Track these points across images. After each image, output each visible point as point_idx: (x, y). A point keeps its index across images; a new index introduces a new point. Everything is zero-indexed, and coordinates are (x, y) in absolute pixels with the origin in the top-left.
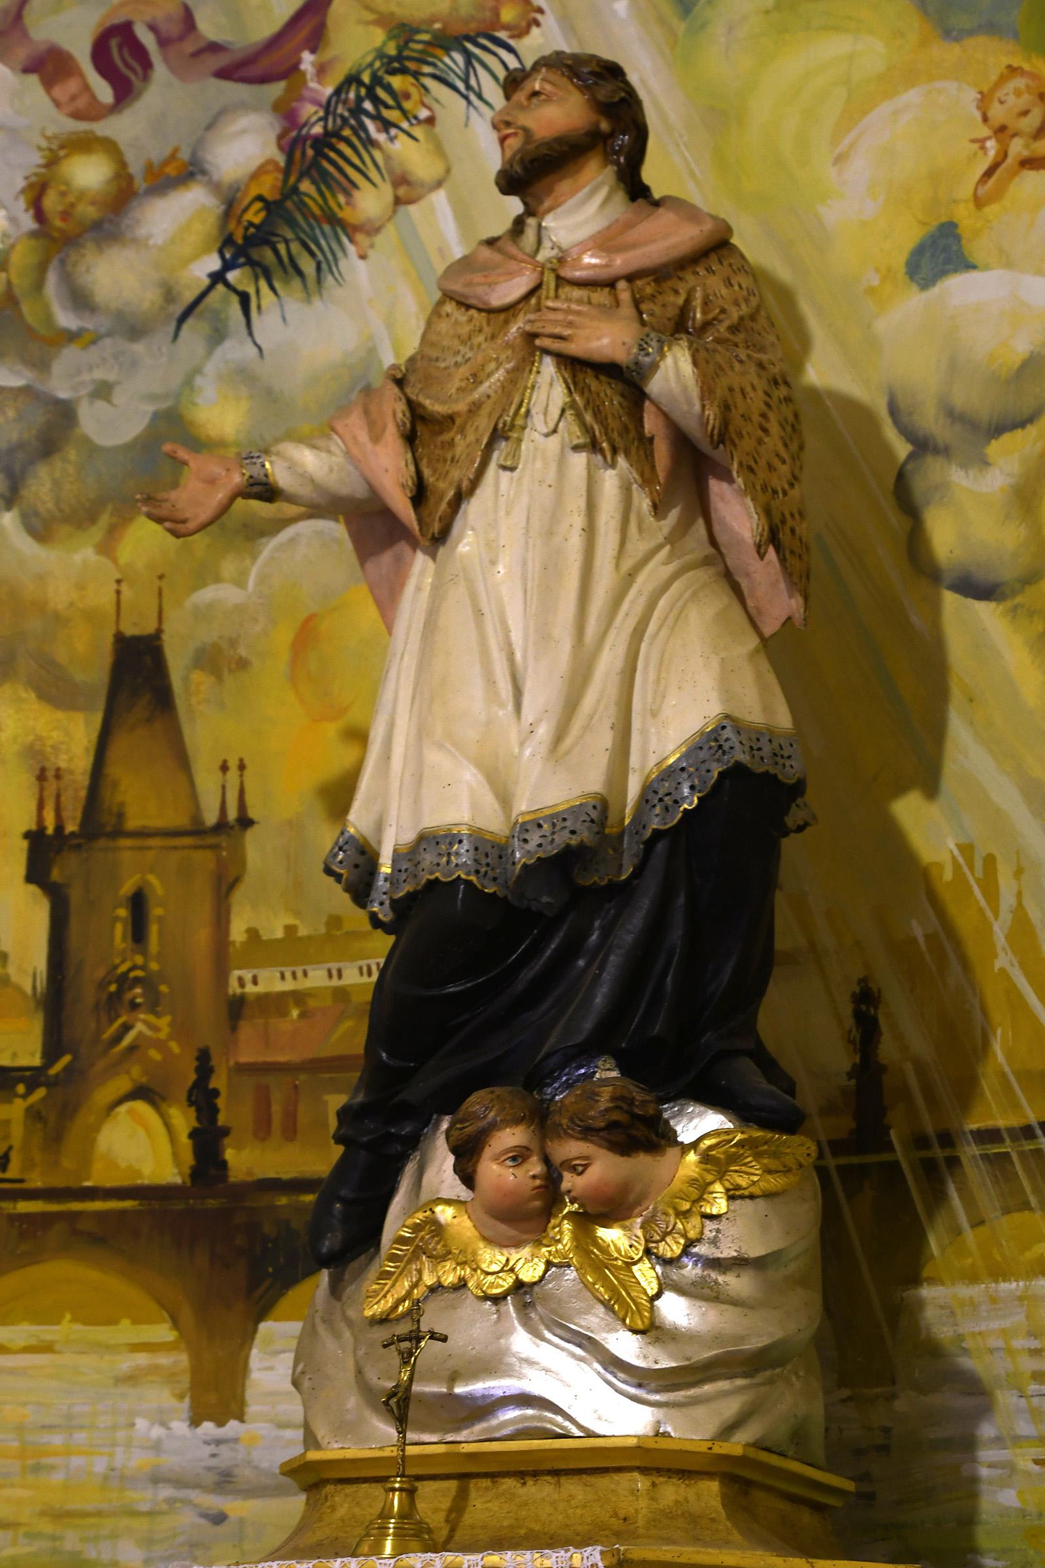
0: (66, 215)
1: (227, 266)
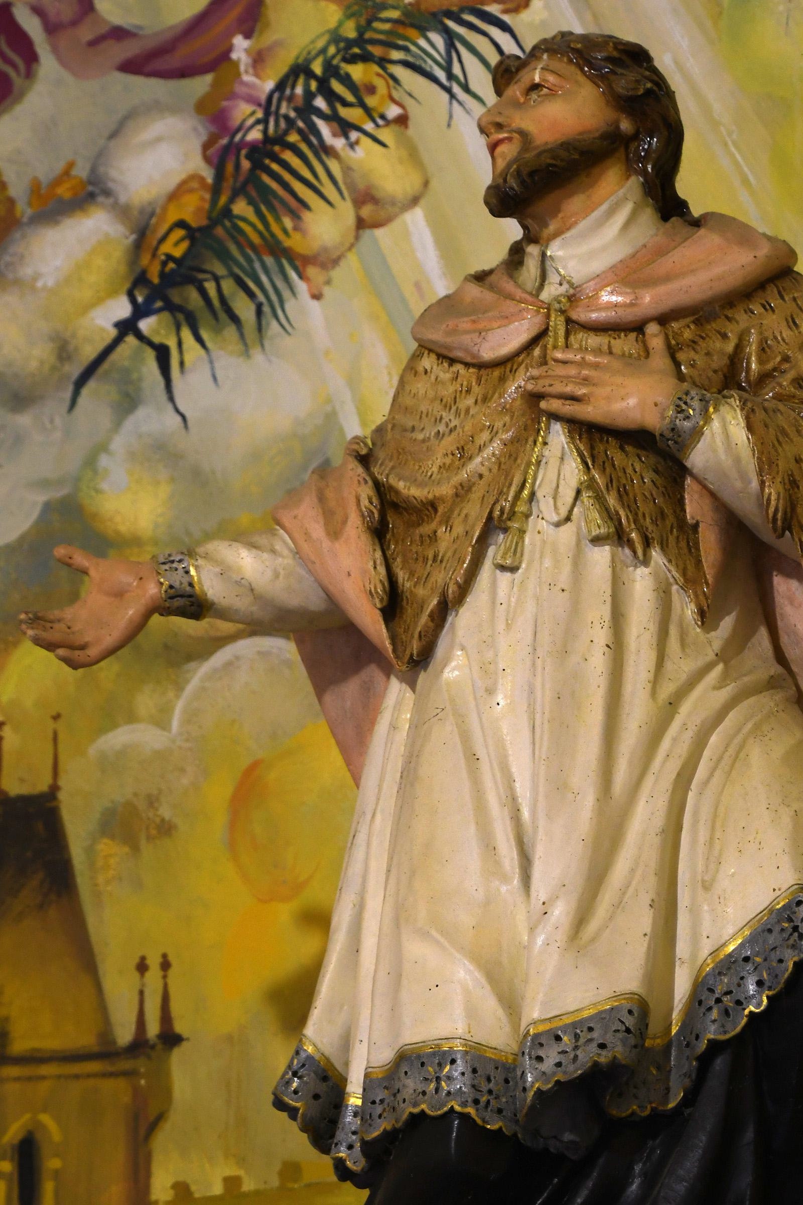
1: (140, 312)
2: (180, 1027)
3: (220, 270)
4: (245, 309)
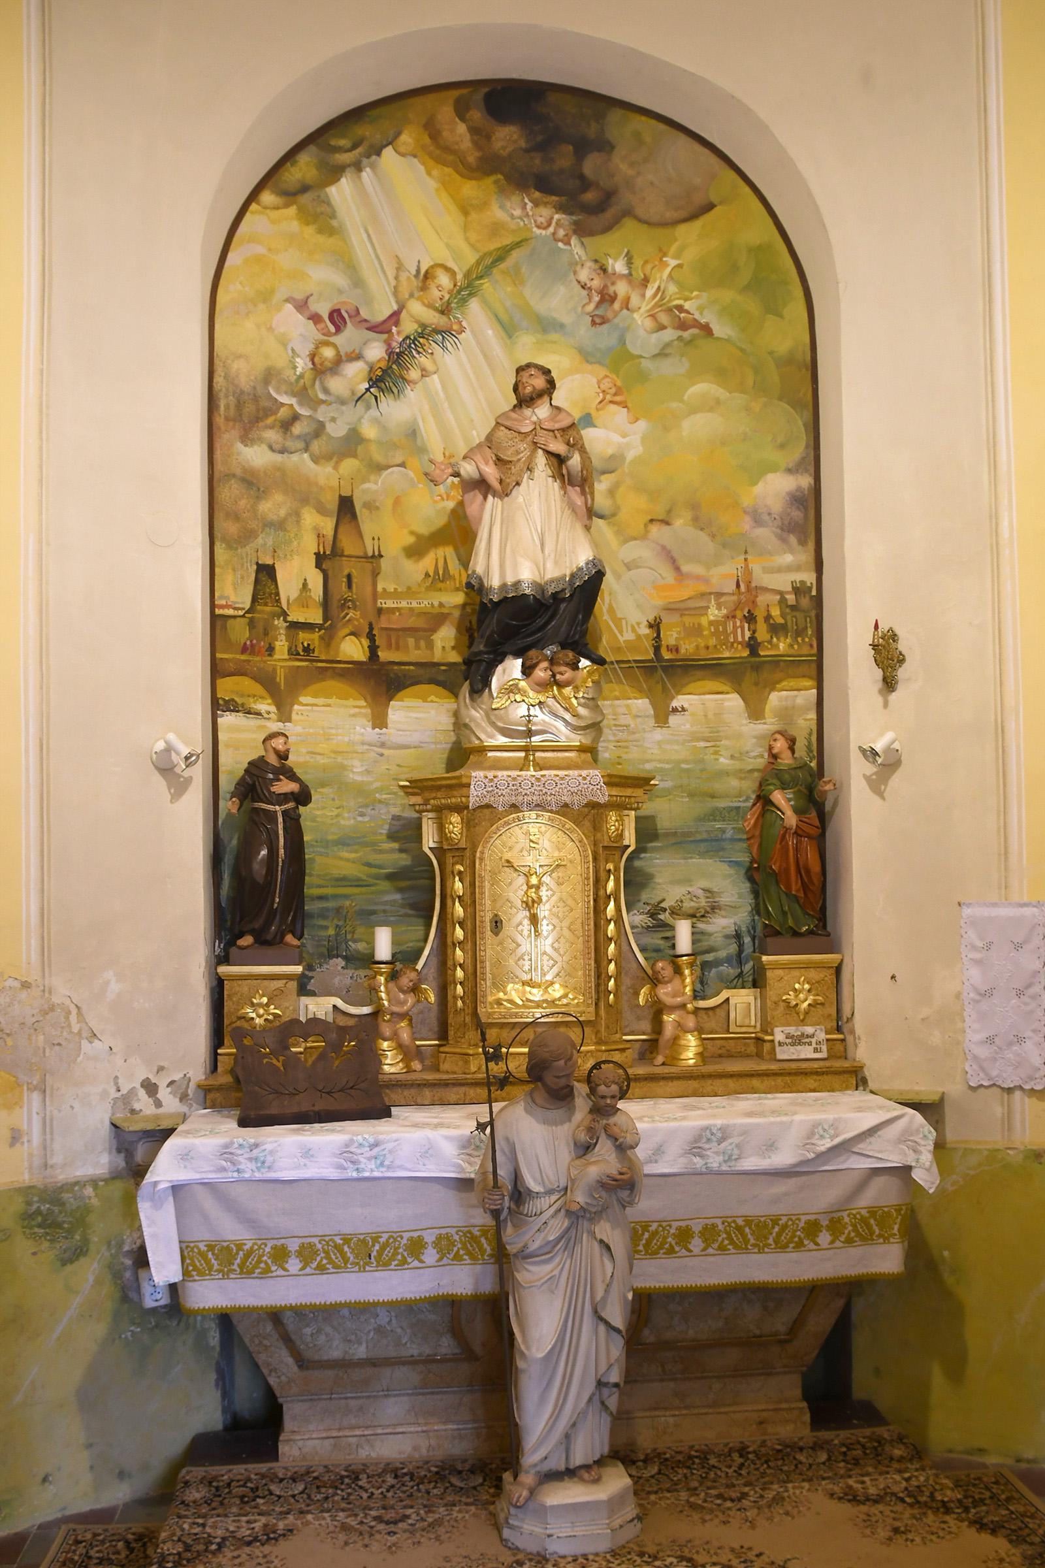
0: (321, 364)
1: (371, 387)
2: (382, 553)
3: (389, 379)
4: (395, 390)
